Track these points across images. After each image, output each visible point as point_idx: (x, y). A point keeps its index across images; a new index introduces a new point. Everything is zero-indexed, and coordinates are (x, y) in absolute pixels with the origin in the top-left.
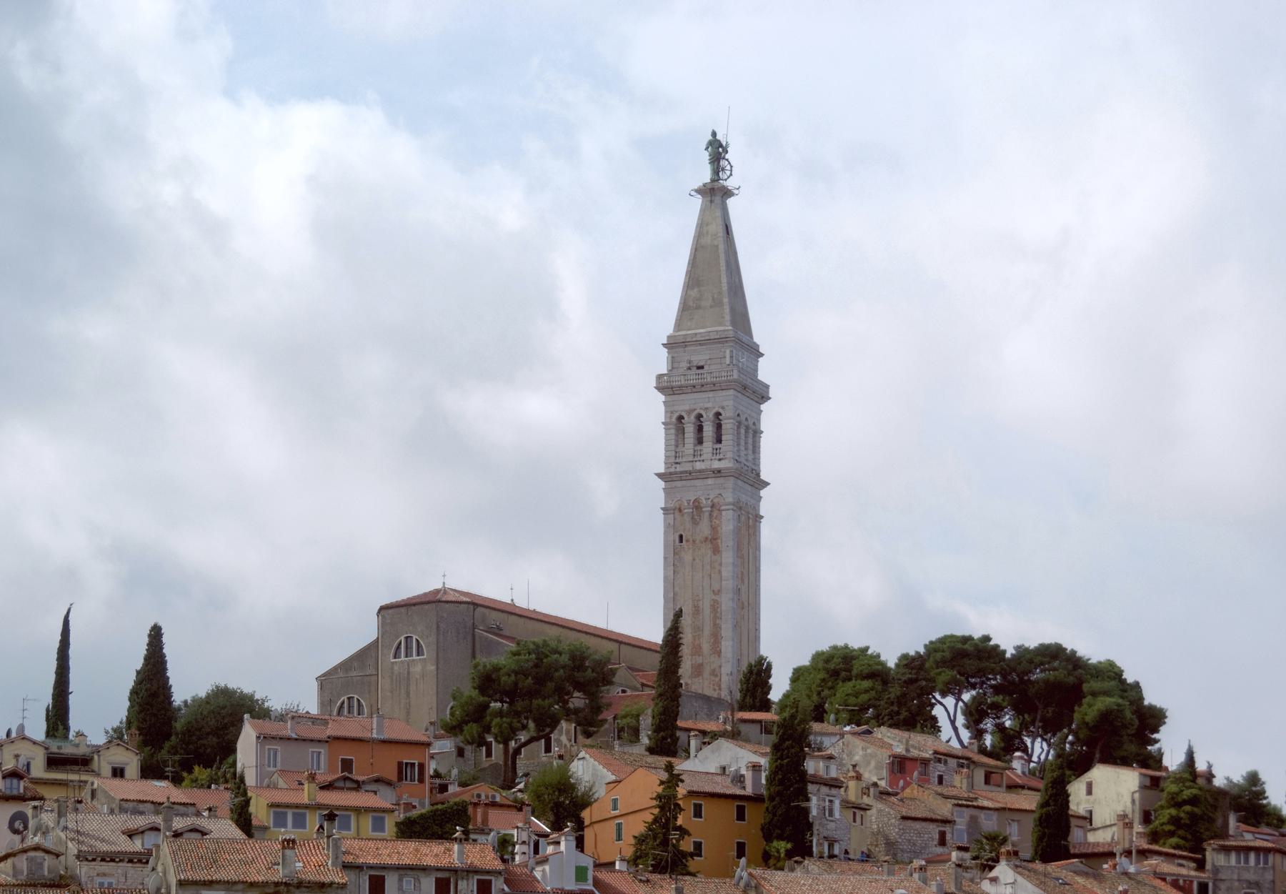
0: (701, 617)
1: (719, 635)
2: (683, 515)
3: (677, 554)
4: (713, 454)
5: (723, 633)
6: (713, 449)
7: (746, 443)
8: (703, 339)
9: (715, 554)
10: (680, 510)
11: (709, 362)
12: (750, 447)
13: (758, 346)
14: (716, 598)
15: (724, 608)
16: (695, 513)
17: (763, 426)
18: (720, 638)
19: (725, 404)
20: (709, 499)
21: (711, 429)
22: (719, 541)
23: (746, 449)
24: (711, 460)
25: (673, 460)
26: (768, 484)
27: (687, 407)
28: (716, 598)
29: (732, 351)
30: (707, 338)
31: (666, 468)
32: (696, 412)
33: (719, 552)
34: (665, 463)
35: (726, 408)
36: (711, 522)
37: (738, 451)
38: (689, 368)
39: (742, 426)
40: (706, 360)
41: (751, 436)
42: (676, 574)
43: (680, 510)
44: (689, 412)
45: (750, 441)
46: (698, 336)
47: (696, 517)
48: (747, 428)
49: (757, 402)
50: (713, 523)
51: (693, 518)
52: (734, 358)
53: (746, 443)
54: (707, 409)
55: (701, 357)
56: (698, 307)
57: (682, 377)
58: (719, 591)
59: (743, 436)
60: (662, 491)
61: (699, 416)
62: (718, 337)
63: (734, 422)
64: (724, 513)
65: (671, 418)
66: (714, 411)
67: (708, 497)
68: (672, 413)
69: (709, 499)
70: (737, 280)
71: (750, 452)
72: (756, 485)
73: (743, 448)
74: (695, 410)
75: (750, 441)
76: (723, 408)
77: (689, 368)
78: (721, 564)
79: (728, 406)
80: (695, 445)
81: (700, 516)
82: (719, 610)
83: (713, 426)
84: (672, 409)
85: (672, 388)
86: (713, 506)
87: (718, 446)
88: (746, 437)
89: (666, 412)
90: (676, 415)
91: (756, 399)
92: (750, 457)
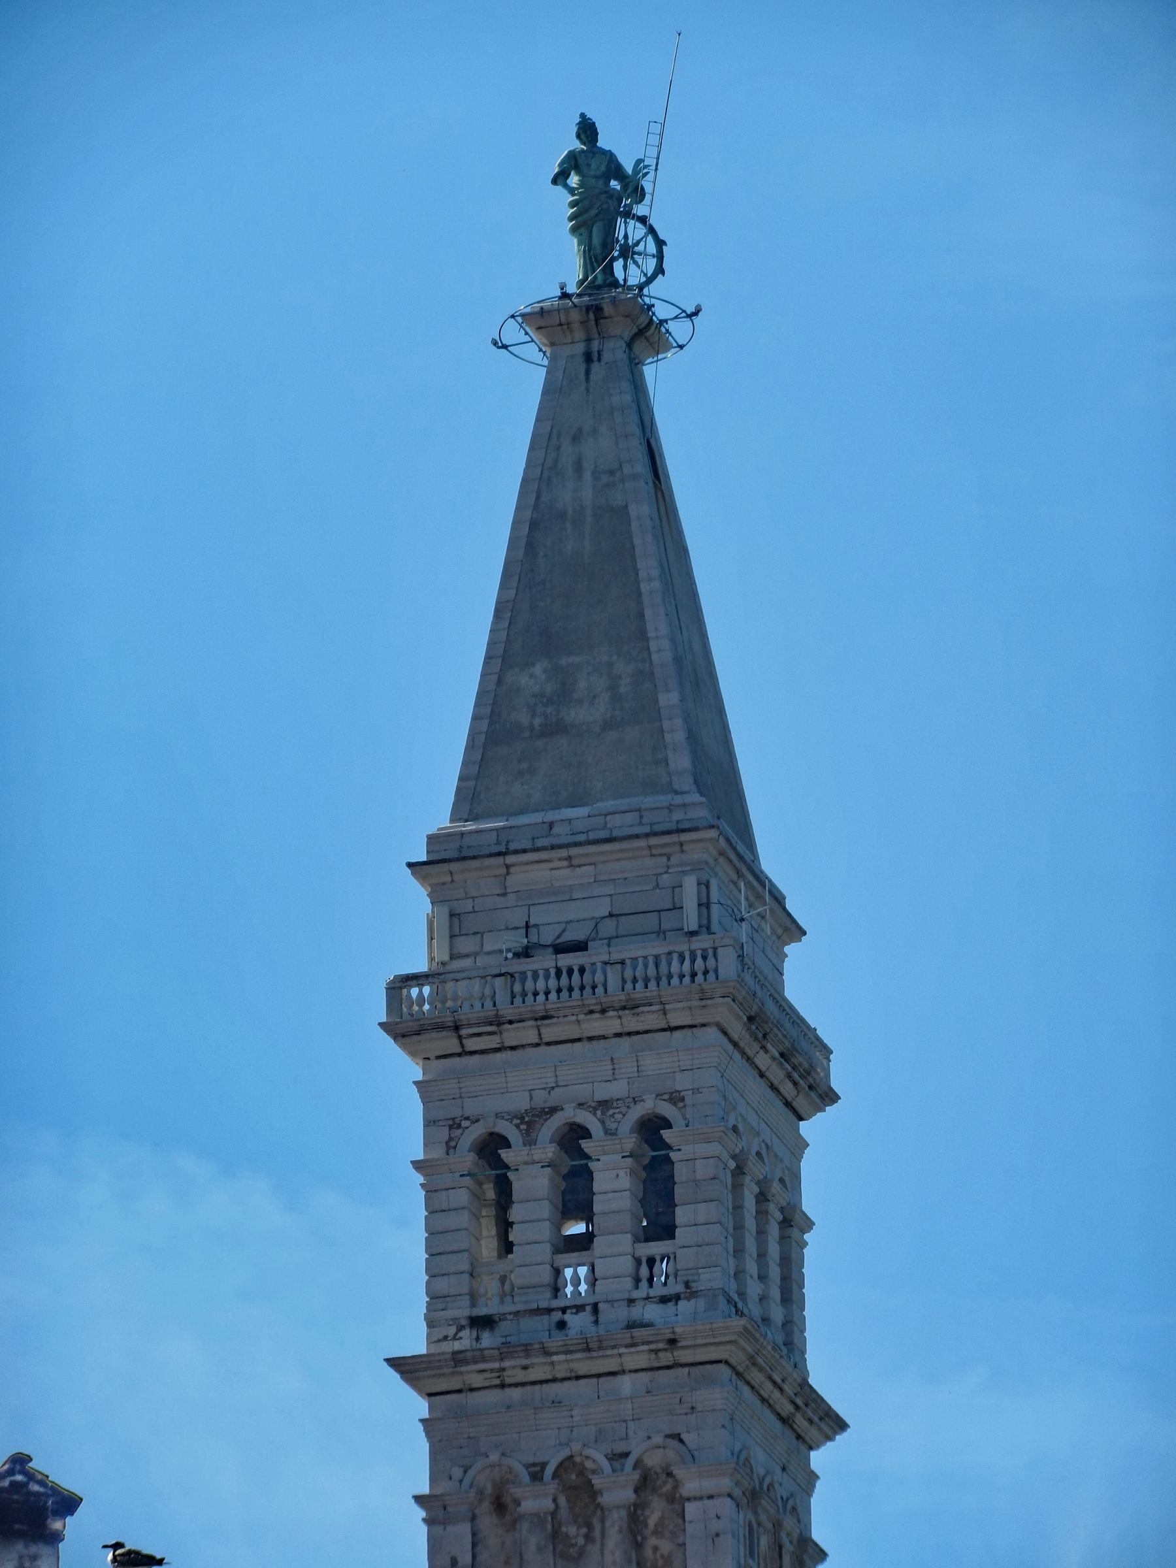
2: (512, 1526)
4: (637, 1280)
6: (638, 1262)
7: (762, 1255)
8: (582, 838)
10: (500, 1506)
11: (608, 928)
12: (775, 1272)
13: (784, 898)
16: (564, 1513)
17: (810, 1203)
19: (683, 1083)
20: (626, 1455)
21: (625, 1181)
23: (762, 1277)
24: (631, 1301)
25: (463, 1311)
26: (840, 1425)
27: (521, 1103)
29: (707, 886)
30: (603, 834)
31: (430, 1341)
32: (556, 1123)
34: (431, 1324)
35: (688, 1096)
36: (638, 1546)
37: (739, 1274)
38: (525, 953)
39: (748, 1179)
40: (598, 921)
41: (774, 1230)
43: (500, 1506)
44: (530, 1121)
45: (774, 1249)
46: (556, 830)
47: (572, 1530)
48: (762, 1197)
49: (788, 1104)
50: (648, 1553)
51: (555, 1535)
52: (715, 910)
53: (762, 1255)
54: (605, 1104)
55: (574, 911)
56: (554, 729)
57: (499, 982)
59: (750, 1224)
60: (420, 1427)
61: (572, 1138)
62: (647, 829)
63: (725, 1156)
64: (691, 1509)
65: (450, 1146)
66: (637, 1112)
67: (621, 1447)
68: (454, 1125)
69: (626, 1455)
70: (697, 647)
71: (775, 1293)
72: (800, 1421)
73: (752, 1268)
74: (553, 1110)
75: (774, 1249)
76: (676, 1099)
77: (525, 953)
79: (696, 1091)
81: (590, 1526)
83: (633, 1173)
84: (457, 1113)
86: (646, 1482)
87: (655, 1248)
88: (761, 1232)
89: (429, 1123)
90: (475, 1133)
91: (788, 1089)
92: (777, 1314)
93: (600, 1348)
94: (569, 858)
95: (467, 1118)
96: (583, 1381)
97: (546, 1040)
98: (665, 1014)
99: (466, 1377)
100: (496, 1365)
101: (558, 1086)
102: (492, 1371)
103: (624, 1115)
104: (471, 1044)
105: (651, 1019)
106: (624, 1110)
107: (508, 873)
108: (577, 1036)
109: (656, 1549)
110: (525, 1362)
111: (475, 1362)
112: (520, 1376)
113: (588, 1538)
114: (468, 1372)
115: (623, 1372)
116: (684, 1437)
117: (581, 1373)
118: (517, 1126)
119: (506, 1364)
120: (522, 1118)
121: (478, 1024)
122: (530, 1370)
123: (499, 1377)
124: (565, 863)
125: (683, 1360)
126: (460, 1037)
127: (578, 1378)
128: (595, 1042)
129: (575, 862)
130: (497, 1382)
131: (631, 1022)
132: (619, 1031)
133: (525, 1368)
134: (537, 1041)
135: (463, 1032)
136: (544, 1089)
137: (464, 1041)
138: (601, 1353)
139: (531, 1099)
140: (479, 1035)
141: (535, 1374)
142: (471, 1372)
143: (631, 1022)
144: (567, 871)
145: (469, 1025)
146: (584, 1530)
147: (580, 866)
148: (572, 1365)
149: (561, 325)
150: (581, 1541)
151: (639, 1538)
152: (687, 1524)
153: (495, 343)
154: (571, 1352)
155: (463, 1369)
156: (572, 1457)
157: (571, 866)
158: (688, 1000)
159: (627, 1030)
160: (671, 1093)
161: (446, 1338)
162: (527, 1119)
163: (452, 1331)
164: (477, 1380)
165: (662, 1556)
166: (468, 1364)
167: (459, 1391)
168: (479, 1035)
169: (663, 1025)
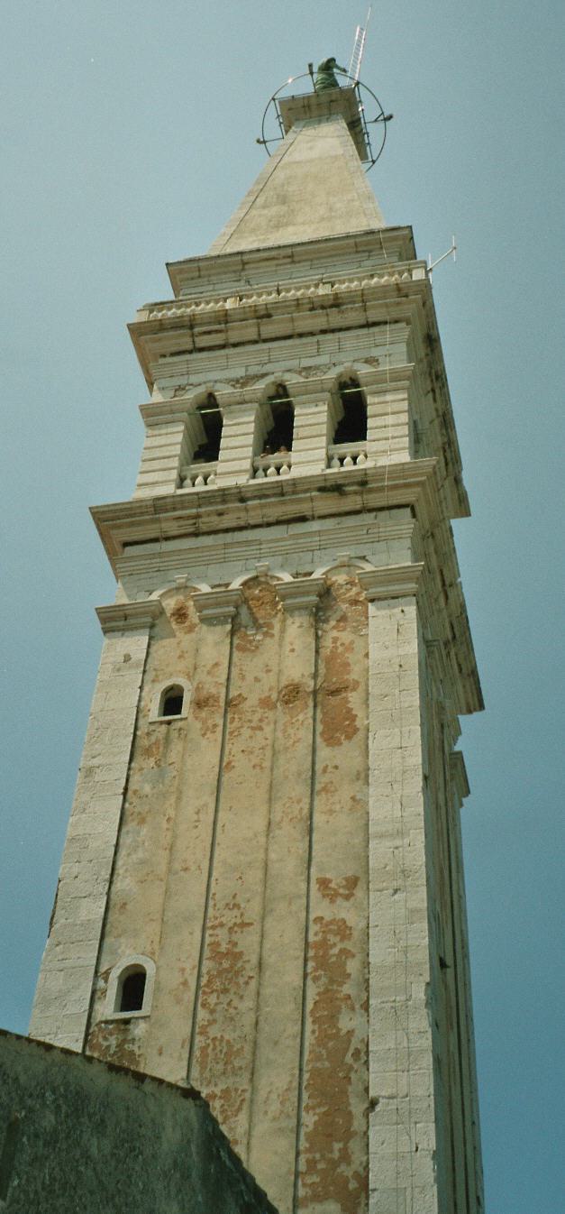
0: (249, 1003)
1: (354, 1089)
3: (148, 752)
5: (380, 1080)
9: (332, 741)
14: (345, 911)
15: (380, 953)
18: (357, 1107)
22: (354, 699)
28: (345, 911)
33: (351, 732)
42: (130, 826)
58: (352, 883)
74: (264, 375)
78: (364, 776)
80: (255, 454)
82: (352, 966)
85: (192, 327)
93: (294, 493)
94: (291, 256)
95: (191, 385)
97: (263, 336)
98: (365, 311)
99: (163, 525)
100: (194, 511)
101: (270, 362)
102: (189, 517)
103: (325, 373)
104: (203, 341)
107: (243, 269)
108: (289, 332)
109: (335, 640)
110: (220, 507)
112: (216, 522)
114: (167, 519)
119: (202, 510)
120: (237, 381)
121: (209, 323)
122: (225, 517)
123: (195, 524)
126: (193, 335)
129: (296, 259)
131: (336, 319)
132: (324, 327)
133: (220, 514)
134: (255, 337)
135: (197, 330)
137: (196, 339)
139: (247, 370)
140: (209, 333)
141: (228, 521)
142: (167, 519)
145: (201, 325)
147: (299, 262)
148: (265, 511)
149: (304, 107)
151: (320, 632)
152: (370, 619)
153: (258, 141)
154: (266, 496)
156: (257, 577)
157: (293, 262)
159: (334, 325)
164: (173, 528)
165: (342, 644)
166: (167, 511)
167: (155, 540)
168: (209, 333)
169: (363, 321)
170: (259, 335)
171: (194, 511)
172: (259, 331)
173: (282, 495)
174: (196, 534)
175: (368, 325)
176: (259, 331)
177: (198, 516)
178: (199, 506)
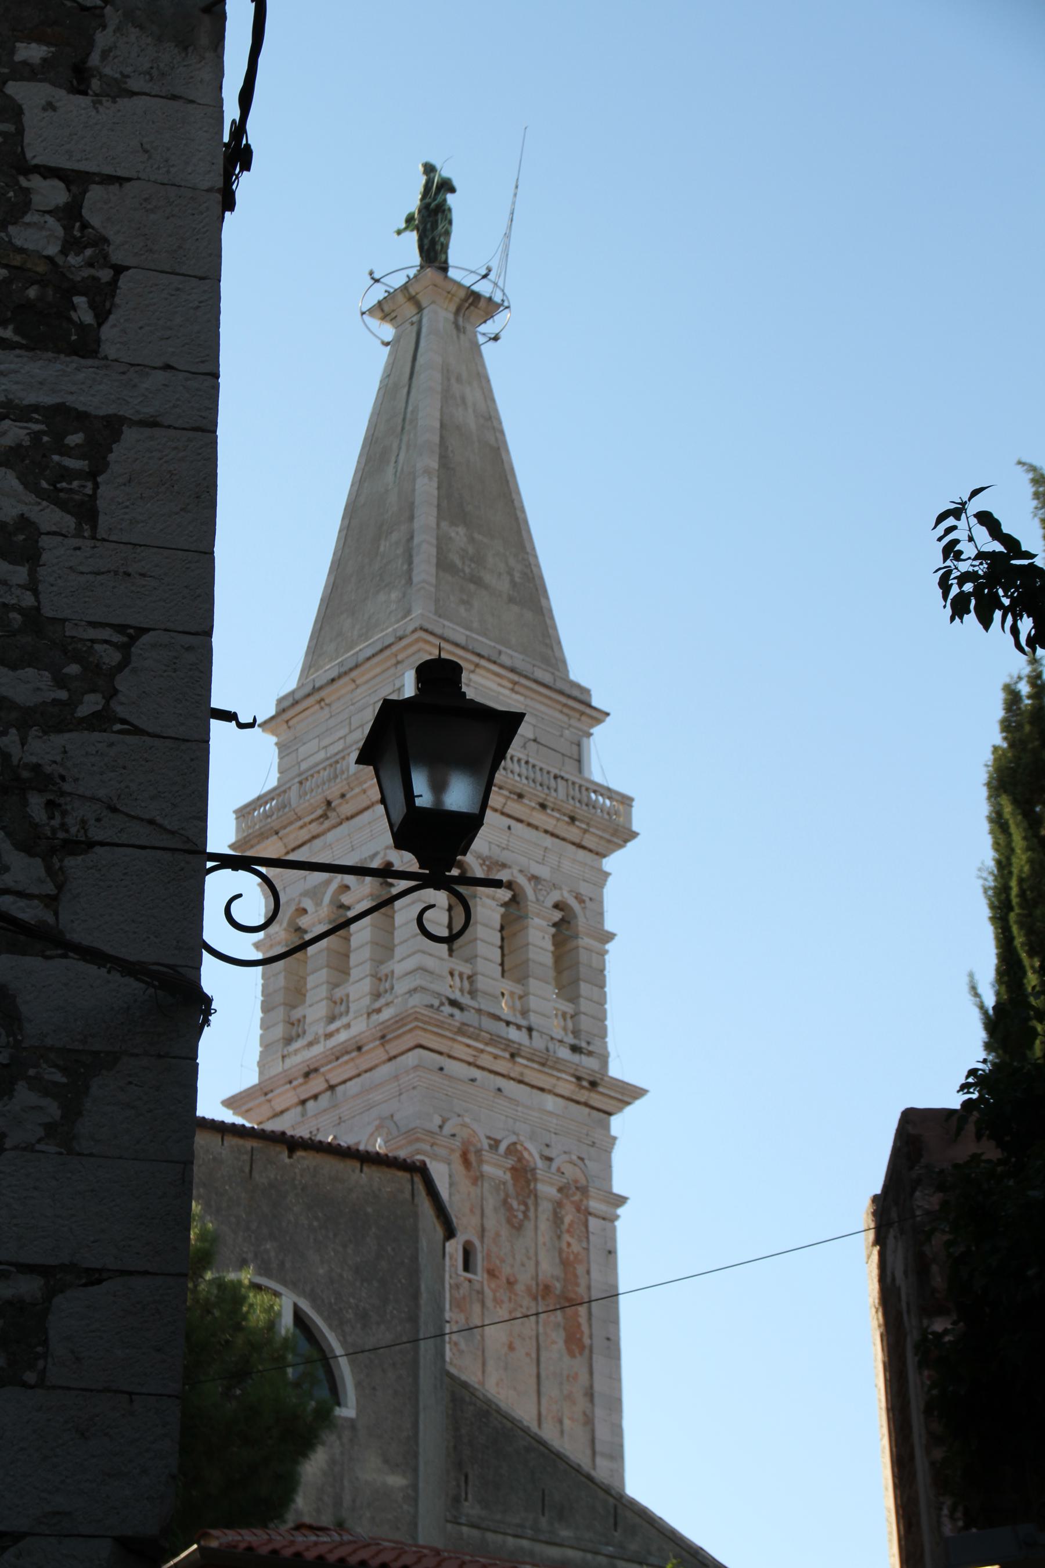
47: (515, 1204)
94: (515, 683)
96: (522, 1086)
97: (505, 810)
100: (481, 1046)
101: (508, 849)
102: (476, 1049)
105: (573, 833)
106: (548, 890)
111: (470, 1037)
113: (525, 1213)
115: (550, 1092)
116: (586, 1161)
117: (526, 1080)
118: (481, 865)
119: (489, 1049)
122: (498, 1061)
123: (475, 1056)
124: (510, 686)
125: (592, 1103)
127: (520, 1082)
128: (530, 828)
130: (471, 1059)
131: (564, 830)
132: (550, 828)
136: (498, 846)
138: (550, 1071)
143: (564, 830)
144: (507, 692)
146: (522, 1208)
148: (527, 1071)
149: (449, 293)
150: (521, 1216)
154: (532, 1061)
155: (460, 1038)
157: (512, 690)
158: (604, 830)
159: (557, 832)
160: (577, 894)
161: (432, 1006)
162: (487, 863)
163: (436, 1003)
167: (441, 1053)
169: (577, 841)
170: (503, 807)
171: (481, 1046)
172: (505, 804)
173: (543, 1065)
174: (469, 1064)
175: (580, 846)
176: (505, 804)
177: (482, 1051)
178: (487, 1044)
